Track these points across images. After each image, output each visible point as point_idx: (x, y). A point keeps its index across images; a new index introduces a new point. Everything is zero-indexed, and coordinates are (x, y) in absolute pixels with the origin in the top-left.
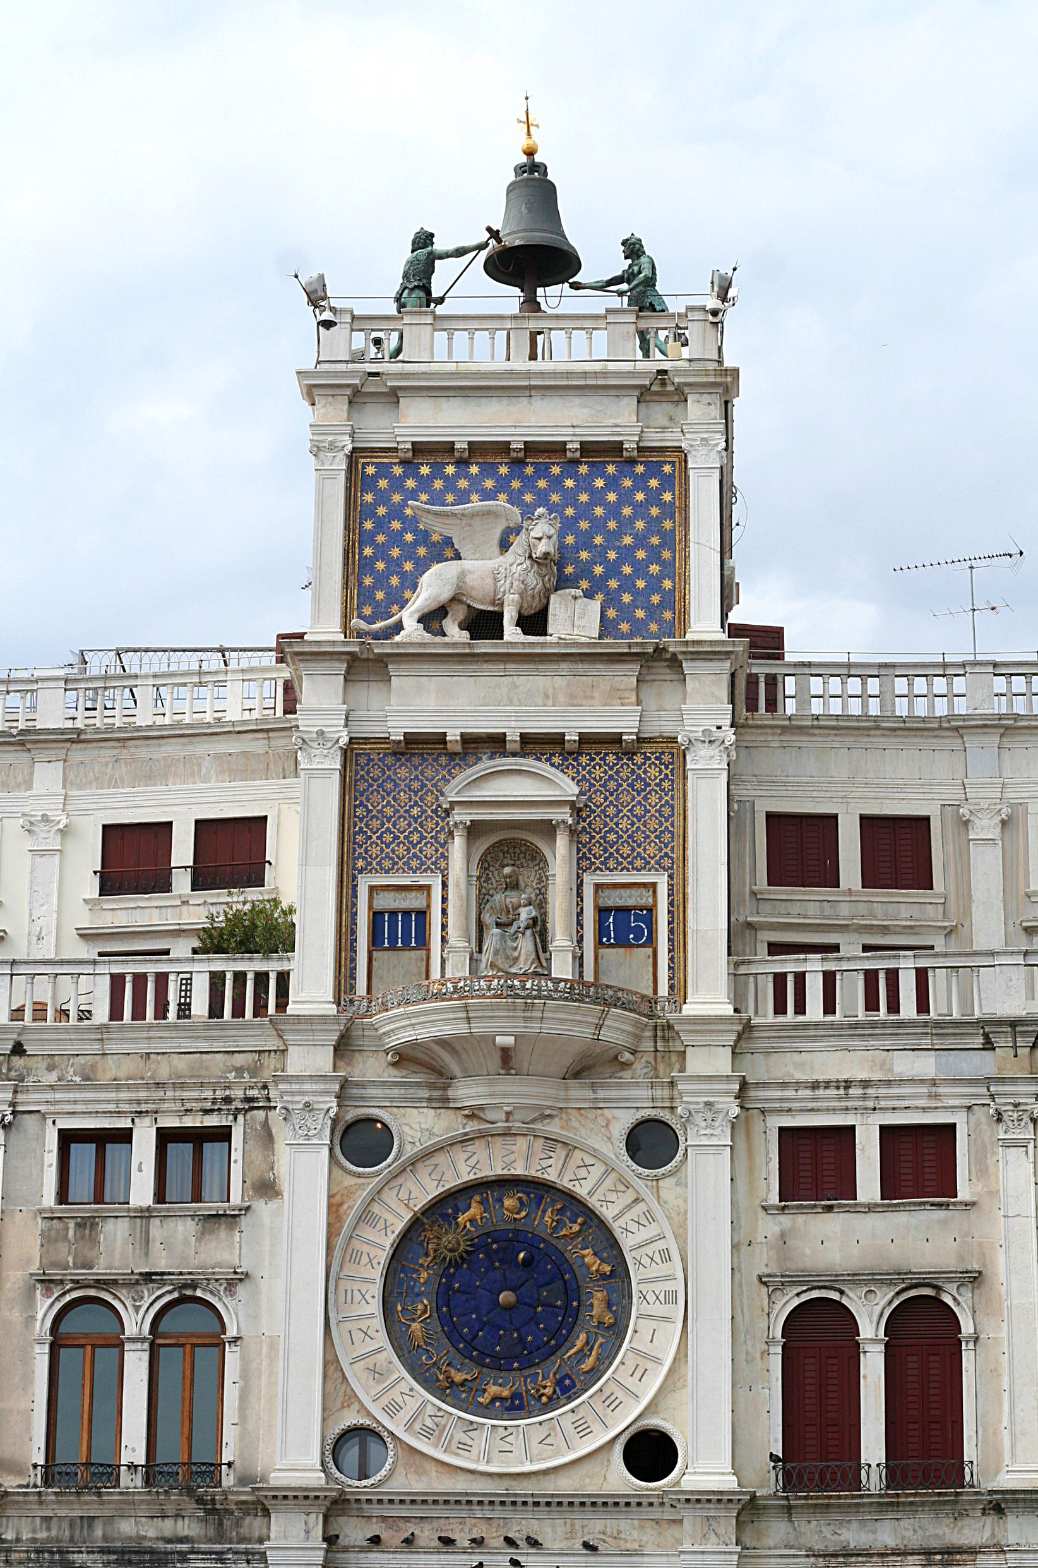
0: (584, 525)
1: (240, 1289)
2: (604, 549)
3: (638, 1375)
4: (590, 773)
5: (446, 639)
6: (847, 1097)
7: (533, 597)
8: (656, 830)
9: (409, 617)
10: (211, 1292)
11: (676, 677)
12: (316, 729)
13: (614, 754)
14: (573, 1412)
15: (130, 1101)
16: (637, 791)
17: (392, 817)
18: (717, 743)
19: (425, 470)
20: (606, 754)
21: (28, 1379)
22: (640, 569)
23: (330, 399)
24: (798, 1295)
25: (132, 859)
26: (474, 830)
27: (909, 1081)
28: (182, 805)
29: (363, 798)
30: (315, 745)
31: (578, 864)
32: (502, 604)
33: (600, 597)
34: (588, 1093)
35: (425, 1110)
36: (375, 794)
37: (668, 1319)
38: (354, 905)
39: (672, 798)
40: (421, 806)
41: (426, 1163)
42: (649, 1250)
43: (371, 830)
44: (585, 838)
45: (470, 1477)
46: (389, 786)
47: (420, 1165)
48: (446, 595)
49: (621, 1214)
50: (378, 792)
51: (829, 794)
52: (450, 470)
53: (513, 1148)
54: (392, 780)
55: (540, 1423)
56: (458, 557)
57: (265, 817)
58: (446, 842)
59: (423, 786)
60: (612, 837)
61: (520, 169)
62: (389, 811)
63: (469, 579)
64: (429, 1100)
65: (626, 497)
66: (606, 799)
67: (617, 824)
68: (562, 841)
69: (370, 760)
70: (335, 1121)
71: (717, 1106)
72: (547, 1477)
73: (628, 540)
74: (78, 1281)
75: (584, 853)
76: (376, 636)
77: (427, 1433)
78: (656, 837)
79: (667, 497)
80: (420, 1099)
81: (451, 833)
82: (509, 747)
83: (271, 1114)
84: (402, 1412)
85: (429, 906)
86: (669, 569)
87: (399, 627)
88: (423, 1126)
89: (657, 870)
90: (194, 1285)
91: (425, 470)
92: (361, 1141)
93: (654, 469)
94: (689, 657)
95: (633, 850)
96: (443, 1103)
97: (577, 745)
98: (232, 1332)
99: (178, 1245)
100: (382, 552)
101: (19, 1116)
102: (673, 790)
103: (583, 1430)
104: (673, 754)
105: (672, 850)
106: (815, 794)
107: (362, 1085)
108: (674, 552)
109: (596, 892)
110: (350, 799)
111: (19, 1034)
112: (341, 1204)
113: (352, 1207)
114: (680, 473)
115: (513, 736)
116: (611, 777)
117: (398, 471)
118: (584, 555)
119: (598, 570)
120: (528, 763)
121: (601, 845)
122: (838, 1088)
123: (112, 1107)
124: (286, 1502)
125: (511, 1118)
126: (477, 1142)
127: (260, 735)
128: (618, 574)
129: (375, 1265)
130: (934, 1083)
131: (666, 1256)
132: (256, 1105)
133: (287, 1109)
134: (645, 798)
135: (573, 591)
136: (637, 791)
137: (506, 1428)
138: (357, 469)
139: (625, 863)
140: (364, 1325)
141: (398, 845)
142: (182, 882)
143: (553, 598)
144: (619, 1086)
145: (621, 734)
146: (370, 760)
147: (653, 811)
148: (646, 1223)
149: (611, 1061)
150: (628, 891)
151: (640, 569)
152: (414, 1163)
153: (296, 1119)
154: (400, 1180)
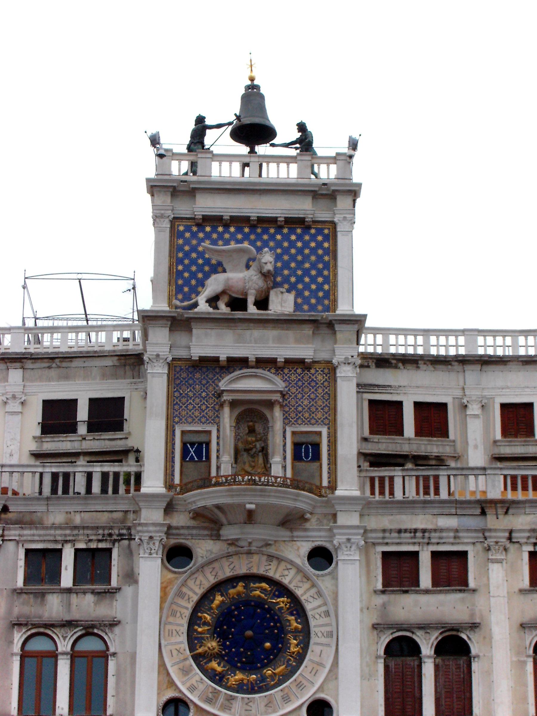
0: (286, 258)
1: (117, 630)
2: (295, 269)
4: (289, 377)
5: (219, 311)
6: (415, 537)
9: (202, 300)
10: (102, 630)
11: (330, 332)
12: (155, 353)
15: (61, 535)
16: (312, 386)
17: (192, 397)
19: (208, 229)
20: (297, 369)
21: (8, 673)
22: (313, 280)
24: (392, 634)
25: (57, 417)
26: (233, 404)
27: (447, 528)
28: (82, 391)
33: (294, 293)
34: (288, 533)
35: (209, 541)
37: (328, 645)
38: (173, 439)
39: (329, 390)
43: (182, 403)
44: (287, 409)
46: (191, 382)
47: (205, 568)
49: (305, 593)
52: (220, 229)
53: (251, 560)
55: (265, 696)
56: (224, 271)
57: (124, 398)
59: (208, 382)
60: (300, 409)
61: (248, 88)
62: (191, 394)
63: (230, 283)
65: (306, 245)
66: (297, 390)
67: (302, 402)
69: (181, 369)
70: (164, 546)
71: (352, 540)
73: (307, 265)
74: (35, 624)
75: (287, 416)
76: (184, 308)
77: (209, 701)
78: (321, 409)
79: (326, 245)
81: (222, 405)
82: (250, 364)
83: (132, 542)
86: (327, 280)
87: (196, 305)
88: (207, 548)
89: (322, 425)
90: (93, 626)
91: (208, 229)
92: (177, 555)
93: (320, 231)
94: (338, 322)
95: (310, 415)
96: (217, 537)
97: (283, 364)
98: (112, 650)
99: (86, 606)
100: (187, 268)
101: (5, 542)
103: (286, 699)
107: (177, 528)
108: (329, 272)
110: (171, 388)
111: (6, 501)
112: (166, 587)
113: (172, 588)
114: (333, 233)
115: (252, 359)
116: (299, 379)
117: (195, 229)
118: (286, 272)
119: (293, 279)
120: (259, 371)
121: (294, 412)
122: (410, 532)
123: (52, 538)
126: (234, 557)
128: (303, 281)
129: (184, 617)
130: (457, 531)
134: (316, 390)
135: (281, 289)
139: (306, 422)
141: (195, 411)
142: (82, 429)
143: (272, 294)
145: (305, 359)
146: (181, 369)
147: (320, 396)
151: (313, 280)
153: (145, 545)
154: (196, 575)
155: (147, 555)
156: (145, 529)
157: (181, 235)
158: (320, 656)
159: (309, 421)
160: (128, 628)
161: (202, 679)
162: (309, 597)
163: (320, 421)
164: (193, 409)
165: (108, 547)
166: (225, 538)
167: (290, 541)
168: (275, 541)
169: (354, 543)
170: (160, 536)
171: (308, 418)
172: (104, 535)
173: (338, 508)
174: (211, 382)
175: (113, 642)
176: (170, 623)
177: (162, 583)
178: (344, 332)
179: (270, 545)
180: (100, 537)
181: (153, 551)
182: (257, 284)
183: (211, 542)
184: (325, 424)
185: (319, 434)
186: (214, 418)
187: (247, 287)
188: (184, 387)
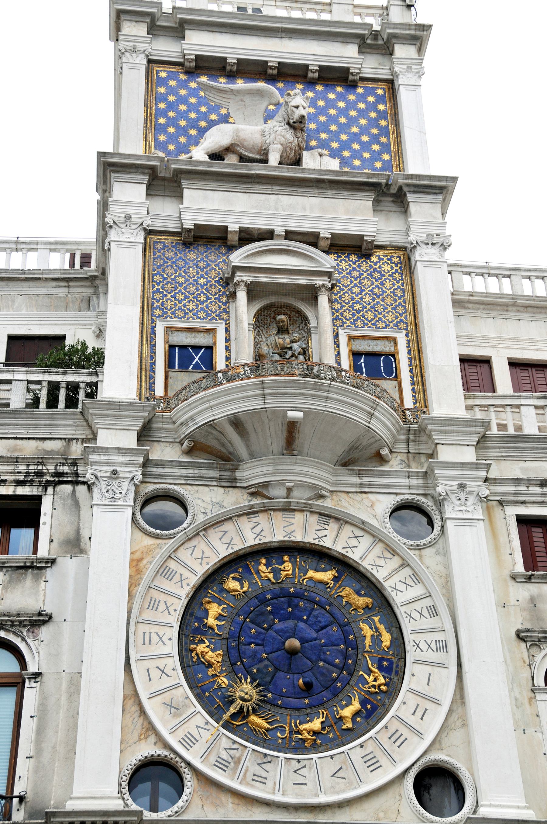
1: (44, 632)
7: (291, 149)
8: (392, 304)
10: (15, 633)
11: (399, 209)
12: (123, 215)
14: (362, 747)
16: (375, 278)
18: (437, 246)
23: (134, 23)
29: (160, 270)
30: (123, 226)
31: (333, 323)
32: (267, 154)
35: (216, 488)
36: (169, 268)
37: (441, 665)
38: (153, 339)
40: (207, 278)
41: (217, 530)
42: (418, 605)
44: (337, 306)
45: (266, 809)
47: (211, 531)
48: (226, 141)
50: (172, 267)
51: (483, 344)
53: (292, 521)
54: (183, 260)
55: (332, 757)
59: (208, 265)
62: (181, 280)
63: (242, 135)
64: (220, 479)
66: (351, 282)
68: (323, 299)
71: (468, 489)
72: (342, 810)
73: (355, 130)
77: (222, 765)
78: (392, 309)
79: (381, 107)
80: (212, 479)
81: (233, 296)
84: (197, 744)
85: (214, 343)
88: (214, 500)
92: (158, 509)
95: (375, 316)
96: (231, 483)
98: (32, 668)
100: (173, 122)
102: (402, 279)
104: (400, 258)
105: (406, 317)
106: (473, 344)
107: (161, 464)
108: (389, 138)
109: (349, 341)
110: (149, 270)
112: (141, 559)
113: (151, 563)
114: (389, 94)
115: (280, 231)
117: (183, 77)
125: (292, 495)
126: (261, 515)
127: (62, 284)
129: (172, 612)
131: (434, 611)
132: (65, 479)
133: (96, 477)
134: (382, 284)
136: (375, 278)
137: (299, 761)
138: (152, 73)
140: (161, 663)
141: (189, 302)
143: (305, 154)
144: (384, 474)
145: (363, 236)
146: (165, 246)
147: (388, 292)
148: (412, 584)
149: (370, 458)
150: (375, 342)
152: (206, 527)
154: (194, 542)
156: (104, 458)
157: (163, 82)
158: (428, 684)
159: (373, 324)
160: (66, 628)
161: (207, 723)
162: (399, 584)
163: (391, 325)
164: (184, 300)
165: (35, 493)
166: (245, 485)
167: (357, 492)
168: (332, 491)
169: (471, 493)
171: (372, 320)
172: (27, 474)
173: (437, 438)
174: (213, 266)
175: (36, 654)
176: (146, 622)
177: (132, 553)
178: (421, 208)
179: (322, 497)
180: (22, 478)
181: (118, 496)
182: (283, 137)
183: (222, 490)
184: (400, 329)
185: (394, 340)
186: (220, 312)
187: (268, 142)
188: (169, 270)
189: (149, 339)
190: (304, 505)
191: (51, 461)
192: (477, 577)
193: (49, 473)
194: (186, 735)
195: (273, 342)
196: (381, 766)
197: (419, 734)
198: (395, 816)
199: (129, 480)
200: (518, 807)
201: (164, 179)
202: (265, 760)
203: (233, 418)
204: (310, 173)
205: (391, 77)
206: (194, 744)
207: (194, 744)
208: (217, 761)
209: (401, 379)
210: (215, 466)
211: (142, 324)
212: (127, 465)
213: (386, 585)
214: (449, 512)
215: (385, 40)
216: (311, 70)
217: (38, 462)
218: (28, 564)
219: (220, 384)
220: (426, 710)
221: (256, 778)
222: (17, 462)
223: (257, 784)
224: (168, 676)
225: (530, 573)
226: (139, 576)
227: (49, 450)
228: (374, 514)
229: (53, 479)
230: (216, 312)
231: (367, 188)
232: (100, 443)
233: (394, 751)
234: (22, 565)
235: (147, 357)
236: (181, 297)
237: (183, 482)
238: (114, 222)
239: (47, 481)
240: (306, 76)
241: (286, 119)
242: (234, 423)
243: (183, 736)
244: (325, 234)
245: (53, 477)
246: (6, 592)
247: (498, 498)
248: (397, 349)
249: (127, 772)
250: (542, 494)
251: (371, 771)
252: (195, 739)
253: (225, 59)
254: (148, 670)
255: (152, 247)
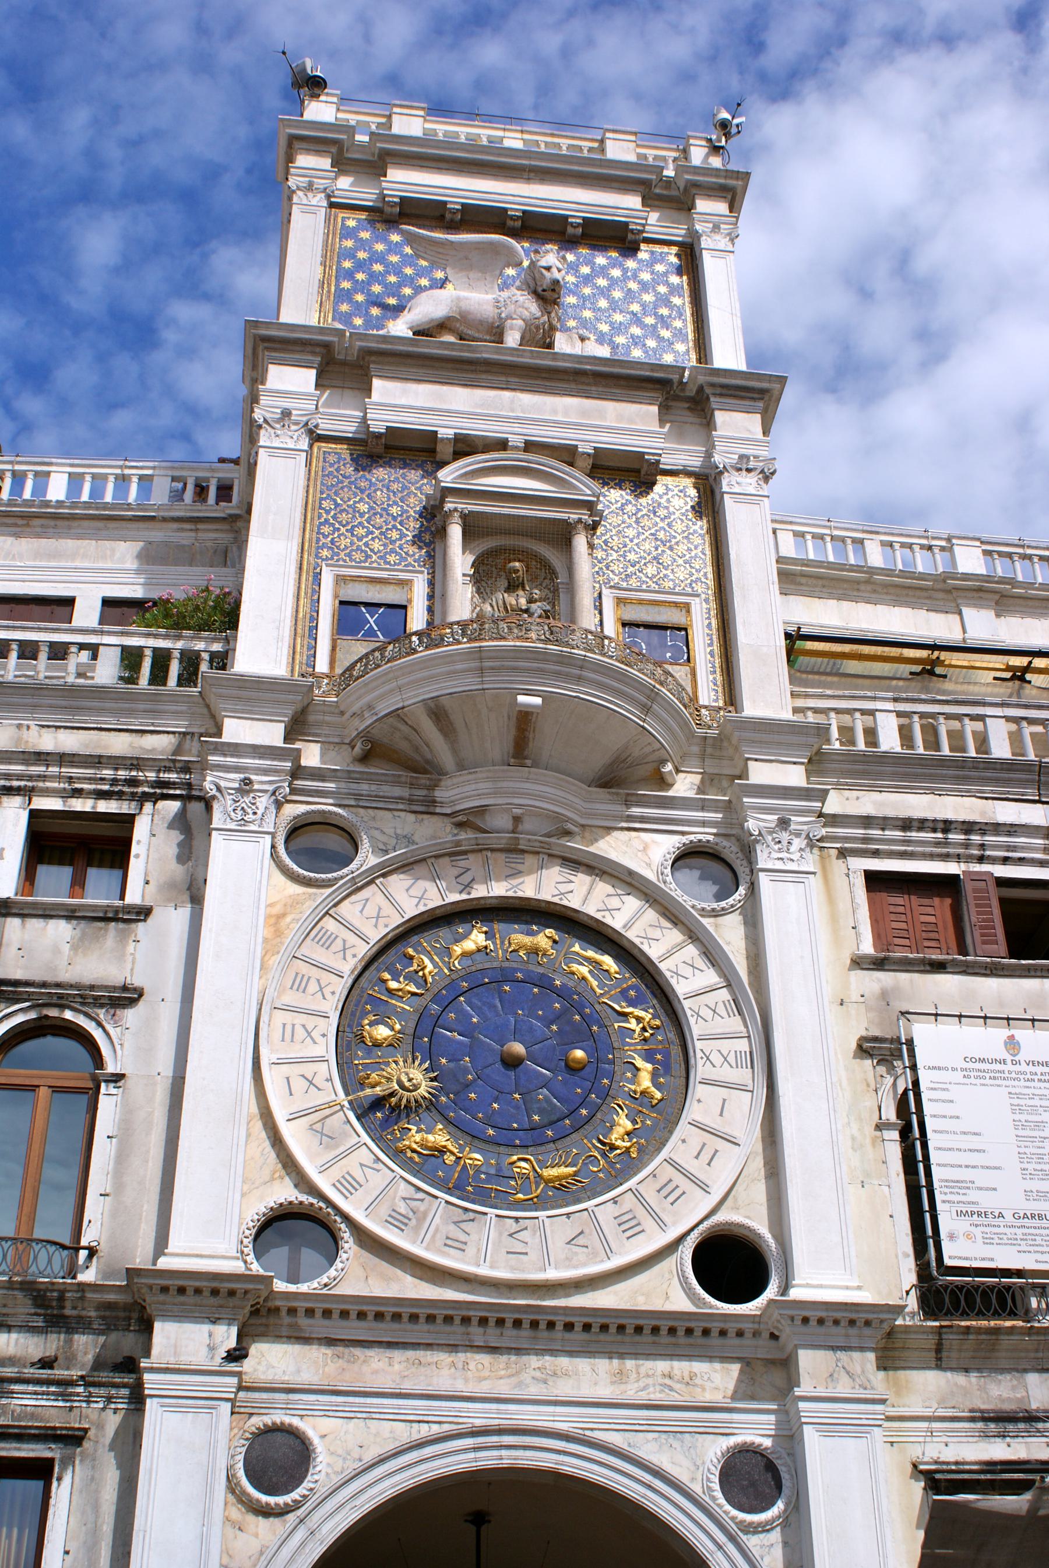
1: (130, 1016)
3: (705, 1156)
6: (946, 843)
10: (87, 1015)
11: (698, 420)
12: (279, 411)
13: (631, 481)
17: (365, 513)
20: (624, 481)
30: (278, 426)
35: (402, 814)
40: (402, 507)
43: (340, 523)
55: (568, 1215)
58: (432, 542)
59: (404, 488)
62: (363, 507)
63: (464, 305)
64: (411, 801)
68: (580, 542)
71: (793, 827)
77: (398, 1221)
81: (442, 533)
84: (361, 1190)
85: (410, 601)
88: (399, 831)
94: (718, 391)
98: (111, 1068)
103: (631, 1227)
110: (315, 490)
124: (182, 1299)
125: (520, 828)
126: (471, 856)
129: (328, 995)
132: (171, 792)
137: (517, 1219)
141: (373, 539)
145: (644, 453)
150: (657, 608)
155: (233, 826)
158: (721, 1115)
162: (681, 966)
164: (367, 536)
166: (448, 811)
168: (583, 826)
170: (270, 782)
171: (654, 576)
179: (568, 833)
180: (106, 787)
181: (250, 817)
183: (412, 817)
185: (687, 607)
188: (346, 494)
189: (310, 591)
190: (538, 844)
191: (151, 763)
192: (802, 957)
193: (147, 782)
194: (343, 1177)
195: (501, 602)
196: (643, 1231)
197: (704, 1188)
198: (662, 1302)
199: (269, 794)
200: (847, 1288)
201: (344, 363)
202: (465, 1217)
203: (432, 705)
204: (565, 361)
205: (689, 240)
206: (356, 1190)
207: (356, 1190)
208: (390, 1216)
209: (695, 664)
210: (403, 779)
211: (301, 568)
212: (266, 772)
213: (663, 966)
214: (763, 860)
215: (682, 189)
216: (572, 223)
217: (132, 764)
218: (110, 915)
219: (415, 651)
220: (716, 1151)
221: (449, 1242)
222: (100, 763)
223: (452, 1251)
224: (319, 1089)
225: (882, 955)
226: (279, 940)
227: (150, 748)
228: (648, 861)
229: (152, 791)
230: (413, 555)
231: (651, 386)
232: (227, 737)
233: (664, 1210)
234: (101, 915)
235: (305, 617)
236: (361, 531)
237: (352, 803)
238: (266, 421)
239: (144, 793)
240: (563, 233)
241: (532, 285)
242: (434, 713)
243: (339, 1177)
244: (585, 448)
245: (153, 787)
246: (76, 954)
247: (838, 845)
248: (691, 620)
249: (251, 1224)
250: (904, 841)
251: (628, 1238)
252: (358, 1183)
253: (445, 203)
254: (288, 1079)
255: (321, 459)
